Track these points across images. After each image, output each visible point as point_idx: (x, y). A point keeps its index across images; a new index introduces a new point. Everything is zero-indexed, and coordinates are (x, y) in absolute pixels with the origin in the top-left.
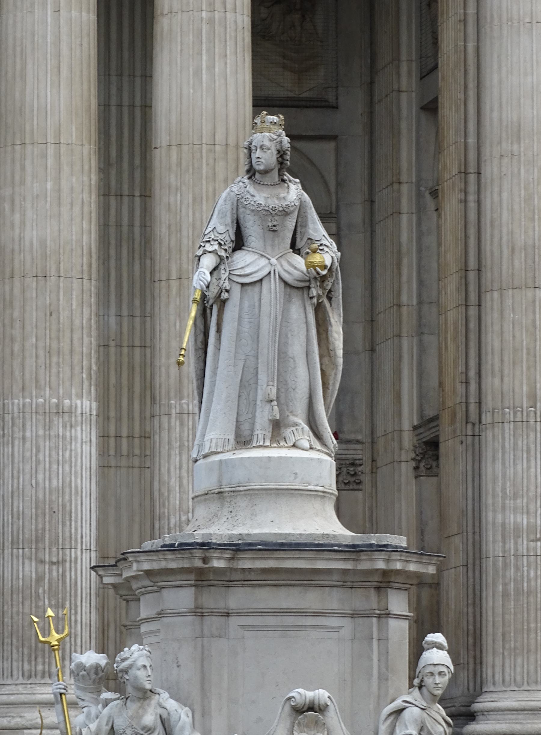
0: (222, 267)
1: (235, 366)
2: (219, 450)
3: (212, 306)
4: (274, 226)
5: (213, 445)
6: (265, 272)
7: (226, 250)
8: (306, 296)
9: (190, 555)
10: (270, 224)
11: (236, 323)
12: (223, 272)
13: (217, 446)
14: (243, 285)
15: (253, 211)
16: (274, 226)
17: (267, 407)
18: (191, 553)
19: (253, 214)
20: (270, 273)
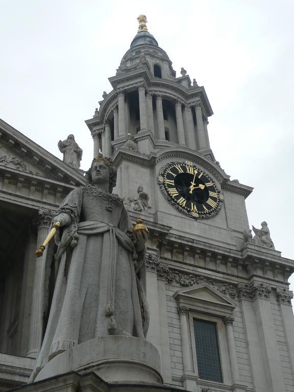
0: (73, 225)
1: (80, 291)
2: (65, 349)
3: (60, 259)
4: (110, 208)
5: (61, 344)
6: (106, 229)
7: (75, 216)
8: (130, 257)
9: (62, 384)
10: (107, 206)
11: (83, 260)
12: (73, 227)
13: (63, 346)
14: (89, 236)
15: (95, 196)
16: (110, 208)
17: (108, 320)
18: (65, 381)
19: (95, 199)
20: (108, 231)
